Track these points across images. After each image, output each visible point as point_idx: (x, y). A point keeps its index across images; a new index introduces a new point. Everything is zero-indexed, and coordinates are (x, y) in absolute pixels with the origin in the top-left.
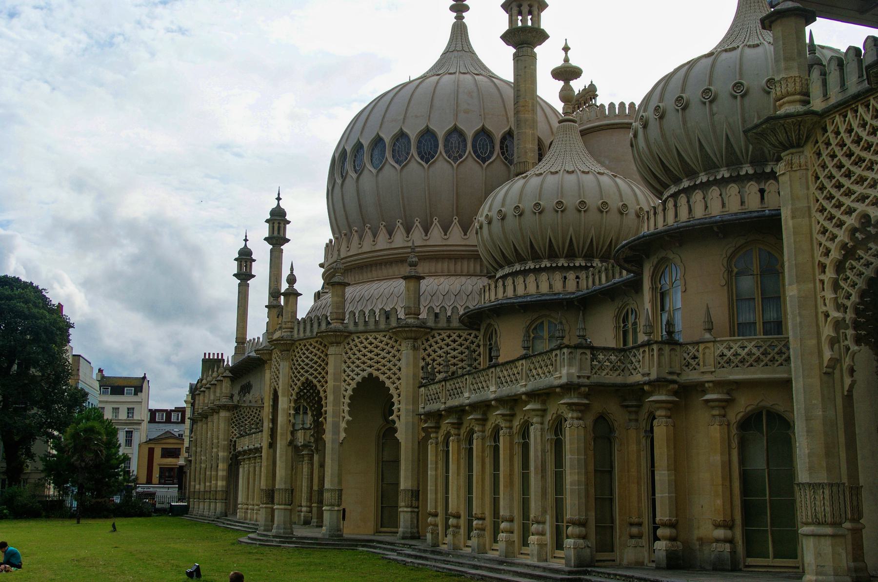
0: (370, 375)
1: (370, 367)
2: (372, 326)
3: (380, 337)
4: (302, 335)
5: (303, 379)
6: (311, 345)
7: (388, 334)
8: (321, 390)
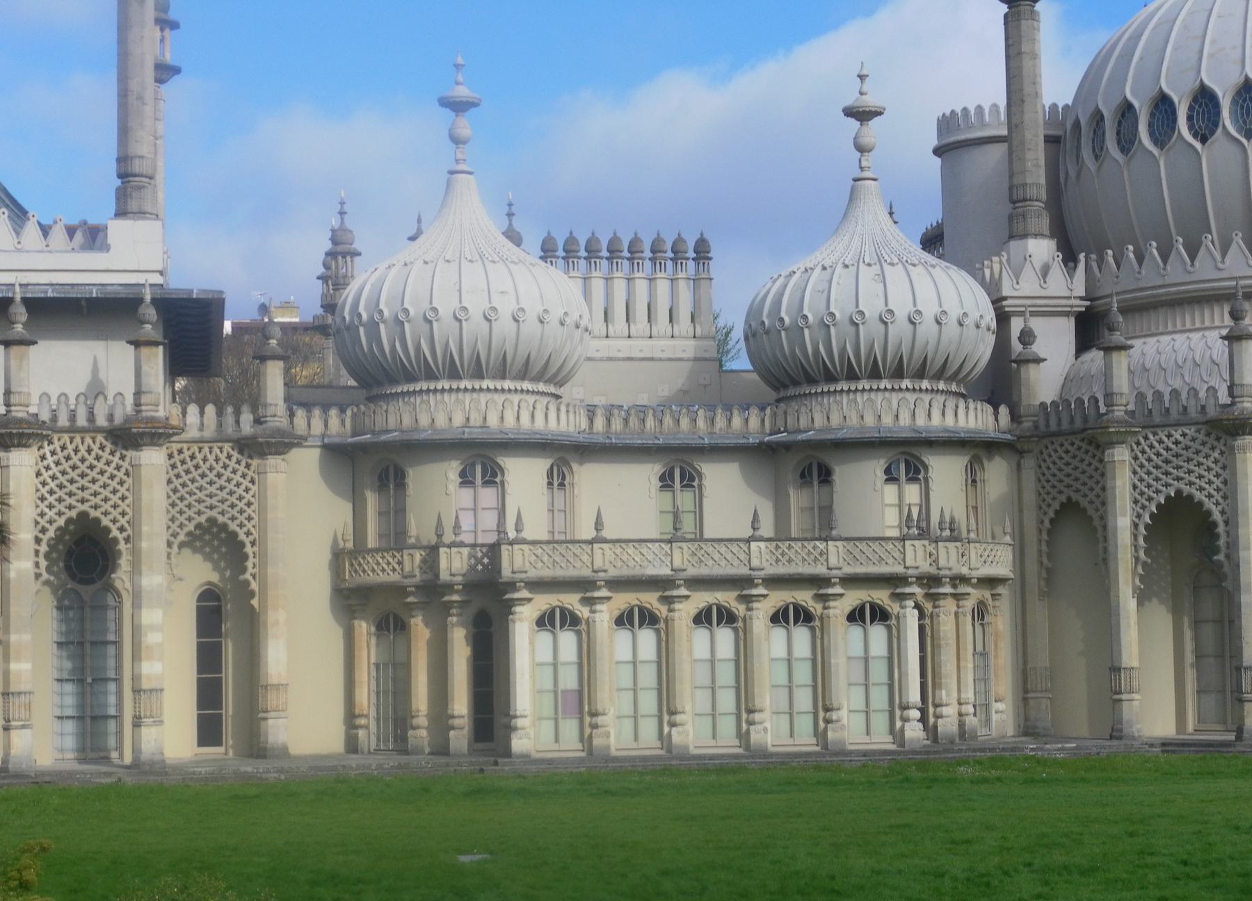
0: (1179, 492)
1: (1178, 479)
2: (1174, 414)
3: (1190, 431)
4: (1053, 427)
5: (1063, 498)
6: (1073, 444)
7: (1204, 428)
8: (1095, 516)
